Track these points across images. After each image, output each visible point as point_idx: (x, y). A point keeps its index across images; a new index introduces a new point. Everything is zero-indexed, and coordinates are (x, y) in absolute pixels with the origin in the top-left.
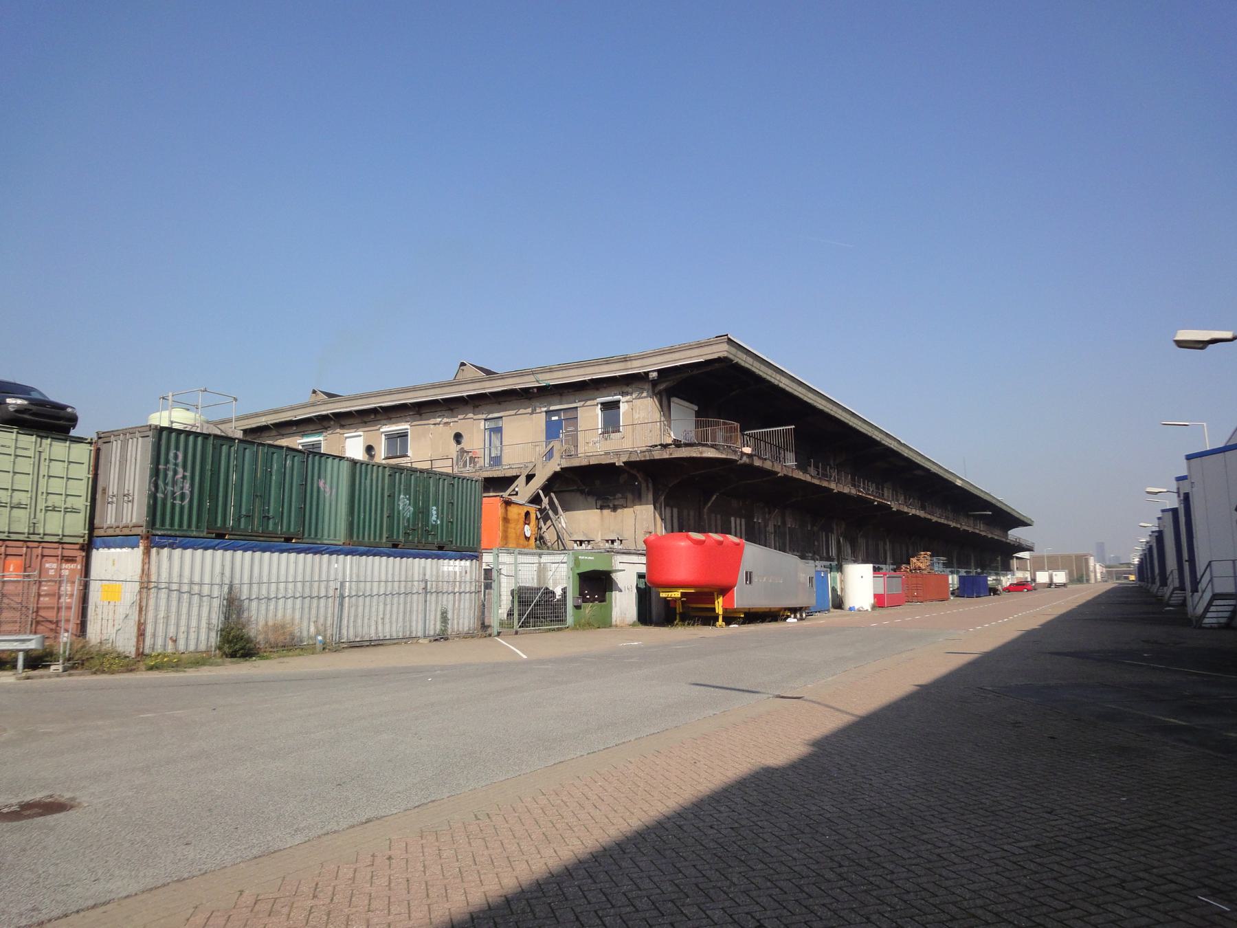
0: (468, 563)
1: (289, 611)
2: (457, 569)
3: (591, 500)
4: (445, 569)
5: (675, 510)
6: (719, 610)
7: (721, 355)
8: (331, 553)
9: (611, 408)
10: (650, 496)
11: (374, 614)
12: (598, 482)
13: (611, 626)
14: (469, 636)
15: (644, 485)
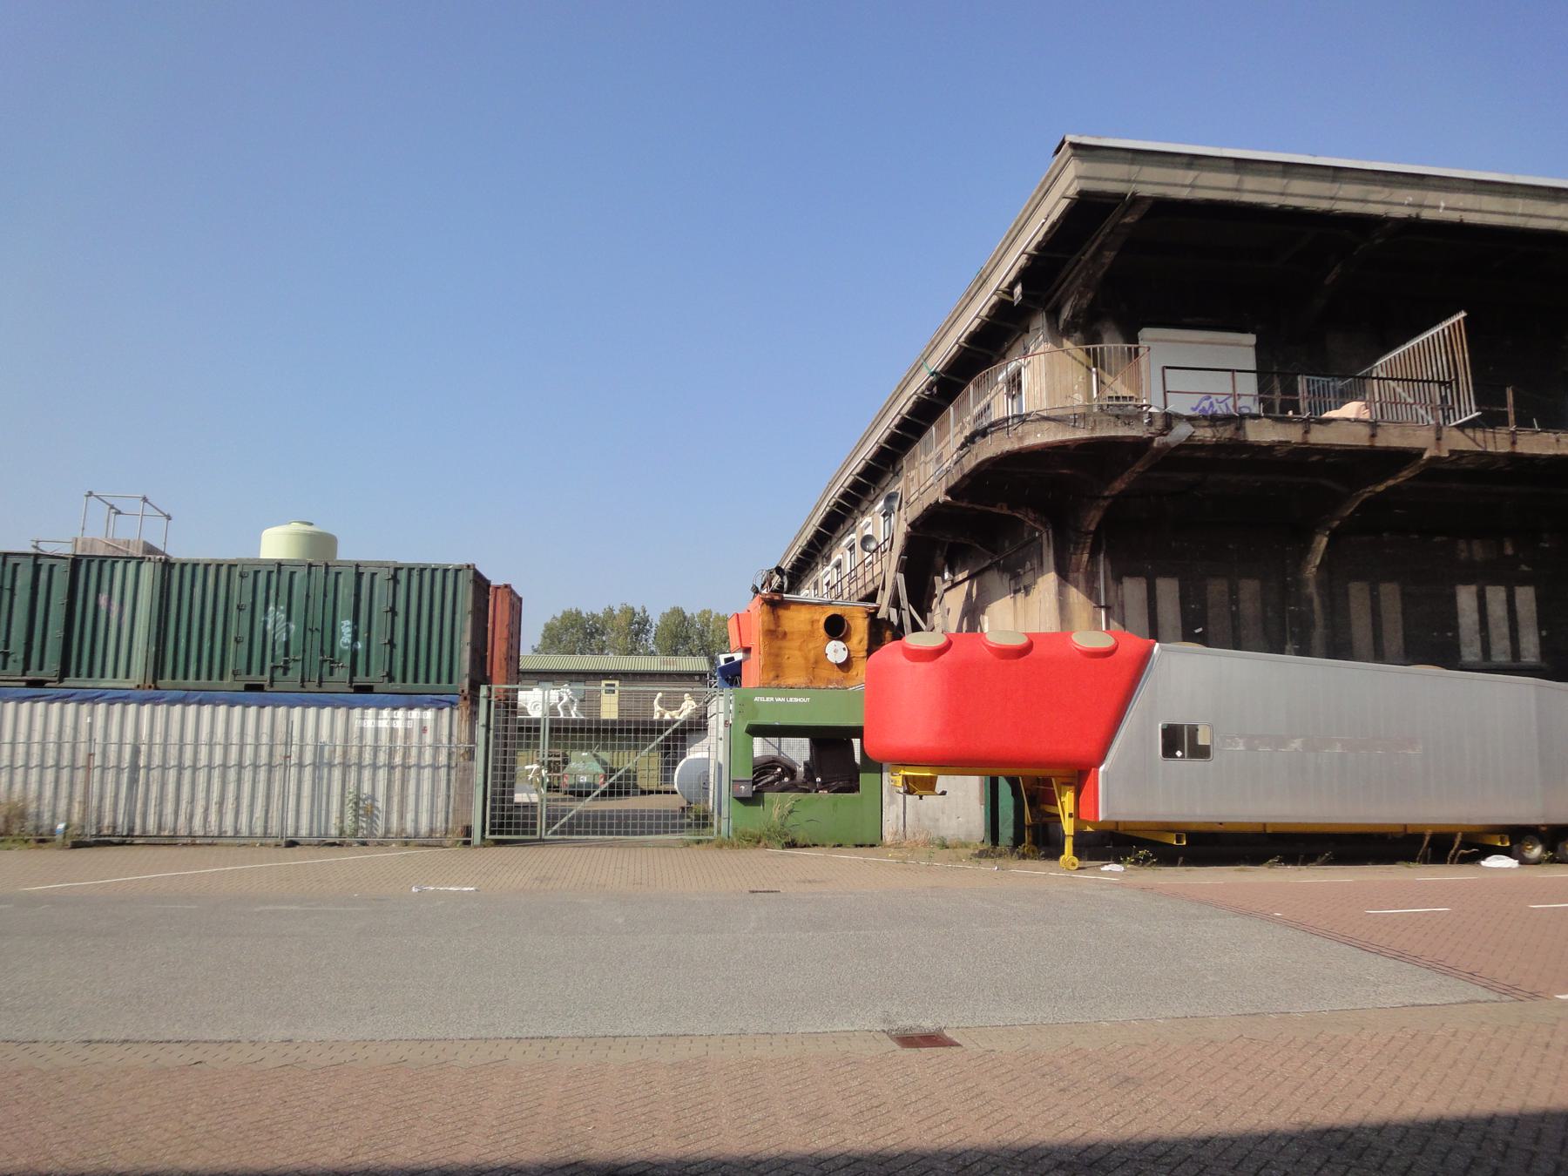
0: (429, 715)
1: (33, 786)
2: (399, 725)
3: (1006, 577)
4: (369, 724)
5: (1168, 589)
6: (1068, 826)
7: (1072, 192)
8: (111, 702)
9: (1015, 383)
10: (1049, 559)
11: (201, 795)
14: (429, 841)
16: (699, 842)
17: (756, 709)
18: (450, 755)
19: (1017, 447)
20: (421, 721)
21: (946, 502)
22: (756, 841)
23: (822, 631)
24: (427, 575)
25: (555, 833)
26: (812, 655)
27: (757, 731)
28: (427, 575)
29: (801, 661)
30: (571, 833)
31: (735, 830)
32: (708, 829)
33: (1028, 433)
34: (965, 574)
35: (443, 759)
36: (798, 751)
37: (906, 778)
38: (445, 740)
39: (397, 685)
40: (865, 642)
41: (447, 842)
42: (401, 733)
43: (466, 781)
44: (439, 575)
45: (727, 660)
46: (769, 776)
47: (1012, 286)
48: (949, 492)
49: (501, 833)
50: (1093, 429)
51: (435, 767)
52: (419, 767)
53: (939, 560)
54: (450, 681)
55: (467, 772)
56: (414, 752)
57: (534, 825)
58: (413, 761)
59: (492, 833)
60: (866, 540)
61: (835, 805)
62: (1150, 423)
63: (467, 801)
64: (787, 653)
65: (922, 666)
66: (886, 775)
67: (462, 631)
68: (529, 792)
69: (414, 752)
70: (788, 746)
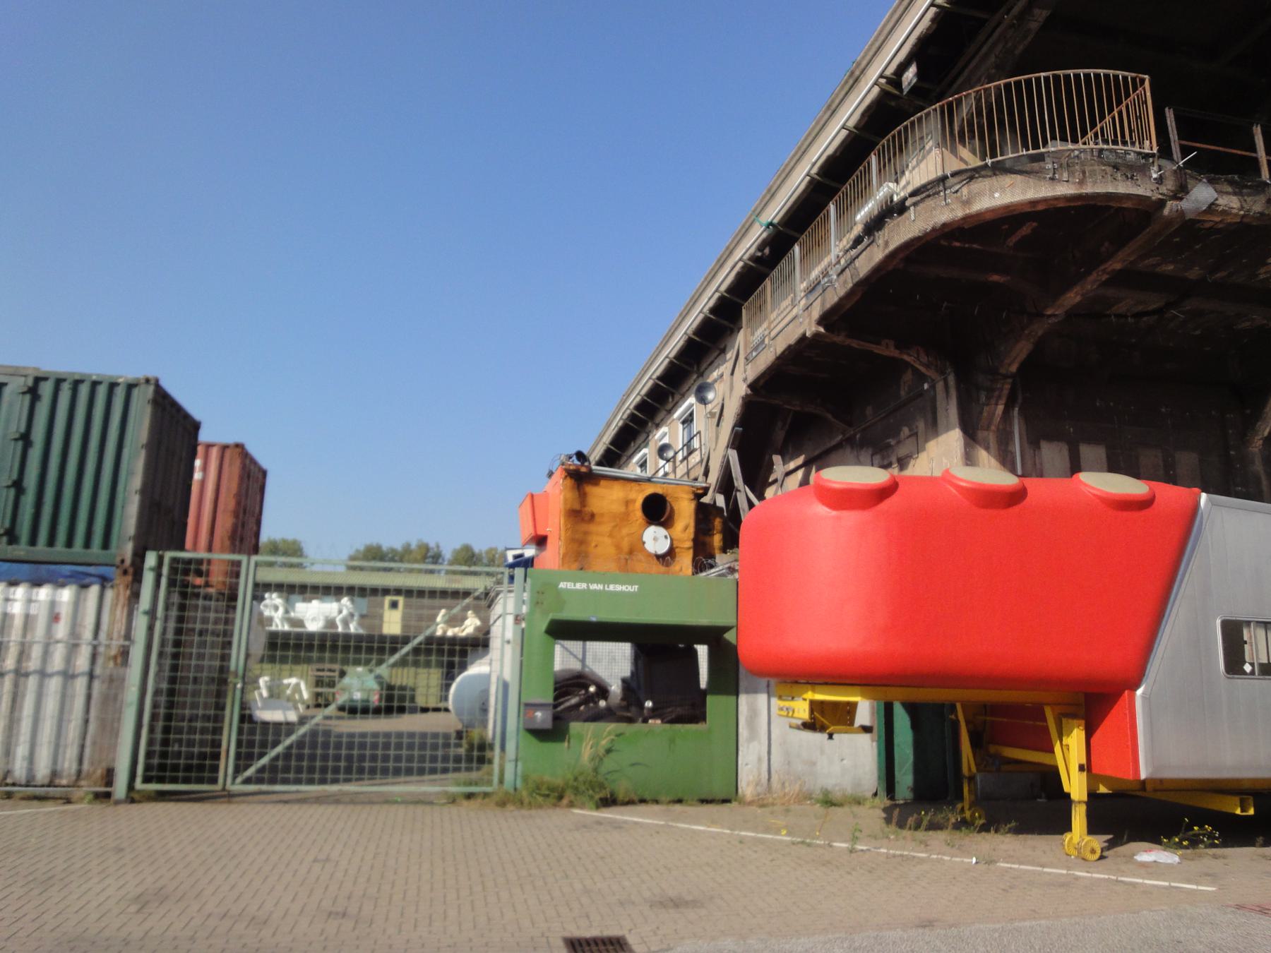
0: (66, 595)
6: (1075, 786)
10: (950, 410)
12: (869, 411)
13: (723, 796)
15: (940, 386)
16: (469, 796)
17: (560, 597)
18: (94, 657)
19: (959, 213)
20: (53, 604)
21: (817, 335)
22: (556, 795)
23: (638, 514)
24: (84, 390)
25: (248, 781)
26: (625, 545)
27: (563, 630)
28: (84, 390)
29: (612, 550)
30: (273, 781)
31: (525, 779)
32: (486, 767)
33: (980, 194)
34: (800, 461)
35: (82, 662)
36: (612, 663)
37: (814, 705)
38: (88, 634)
39: (21, 550)
40: (691, 530)
41: (77, 793)
42: (18, 623)
43: (112, 699)
44: (102, 392)
45: (516, 557)
46: (574, 696)
47: (903, 68)
48: (824, 320)
49: (161, 780)
50: (1082, 183)
51: (68, 676)
52: (43, 674)
53: (779, 435)
54: (106, 545)
55: (115, 682)
56: (36, 652)
57: (215, 769)
58: (33, 664)
59: (147, 780)
60: (662, 450)
61: (672, 741)
62: (1160, 180)
63: (110, 728)
64: (594, 540)
65: (851, 518)
66: (743, 699)
67: (131, 473)
68: (285, 709)
69: (36, 652)
70: (595, 659)
